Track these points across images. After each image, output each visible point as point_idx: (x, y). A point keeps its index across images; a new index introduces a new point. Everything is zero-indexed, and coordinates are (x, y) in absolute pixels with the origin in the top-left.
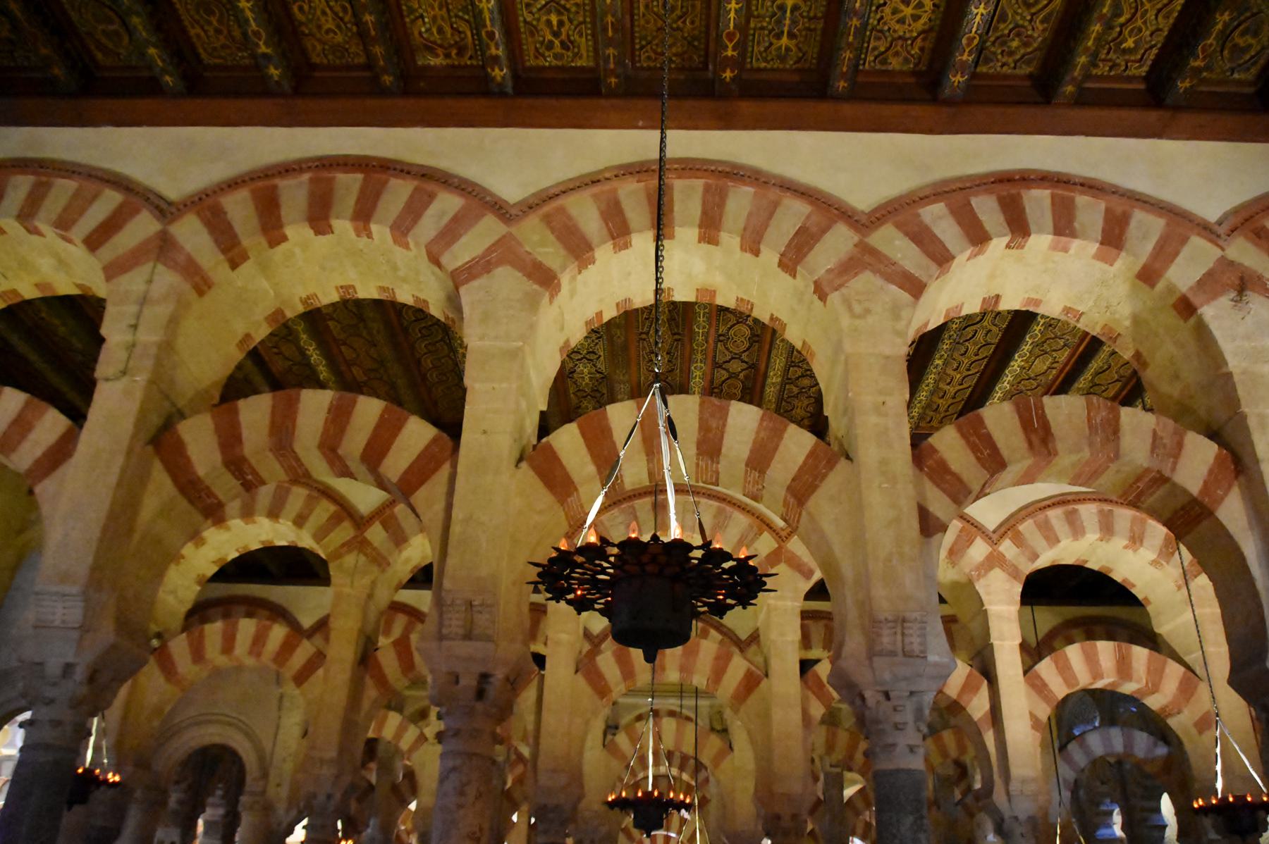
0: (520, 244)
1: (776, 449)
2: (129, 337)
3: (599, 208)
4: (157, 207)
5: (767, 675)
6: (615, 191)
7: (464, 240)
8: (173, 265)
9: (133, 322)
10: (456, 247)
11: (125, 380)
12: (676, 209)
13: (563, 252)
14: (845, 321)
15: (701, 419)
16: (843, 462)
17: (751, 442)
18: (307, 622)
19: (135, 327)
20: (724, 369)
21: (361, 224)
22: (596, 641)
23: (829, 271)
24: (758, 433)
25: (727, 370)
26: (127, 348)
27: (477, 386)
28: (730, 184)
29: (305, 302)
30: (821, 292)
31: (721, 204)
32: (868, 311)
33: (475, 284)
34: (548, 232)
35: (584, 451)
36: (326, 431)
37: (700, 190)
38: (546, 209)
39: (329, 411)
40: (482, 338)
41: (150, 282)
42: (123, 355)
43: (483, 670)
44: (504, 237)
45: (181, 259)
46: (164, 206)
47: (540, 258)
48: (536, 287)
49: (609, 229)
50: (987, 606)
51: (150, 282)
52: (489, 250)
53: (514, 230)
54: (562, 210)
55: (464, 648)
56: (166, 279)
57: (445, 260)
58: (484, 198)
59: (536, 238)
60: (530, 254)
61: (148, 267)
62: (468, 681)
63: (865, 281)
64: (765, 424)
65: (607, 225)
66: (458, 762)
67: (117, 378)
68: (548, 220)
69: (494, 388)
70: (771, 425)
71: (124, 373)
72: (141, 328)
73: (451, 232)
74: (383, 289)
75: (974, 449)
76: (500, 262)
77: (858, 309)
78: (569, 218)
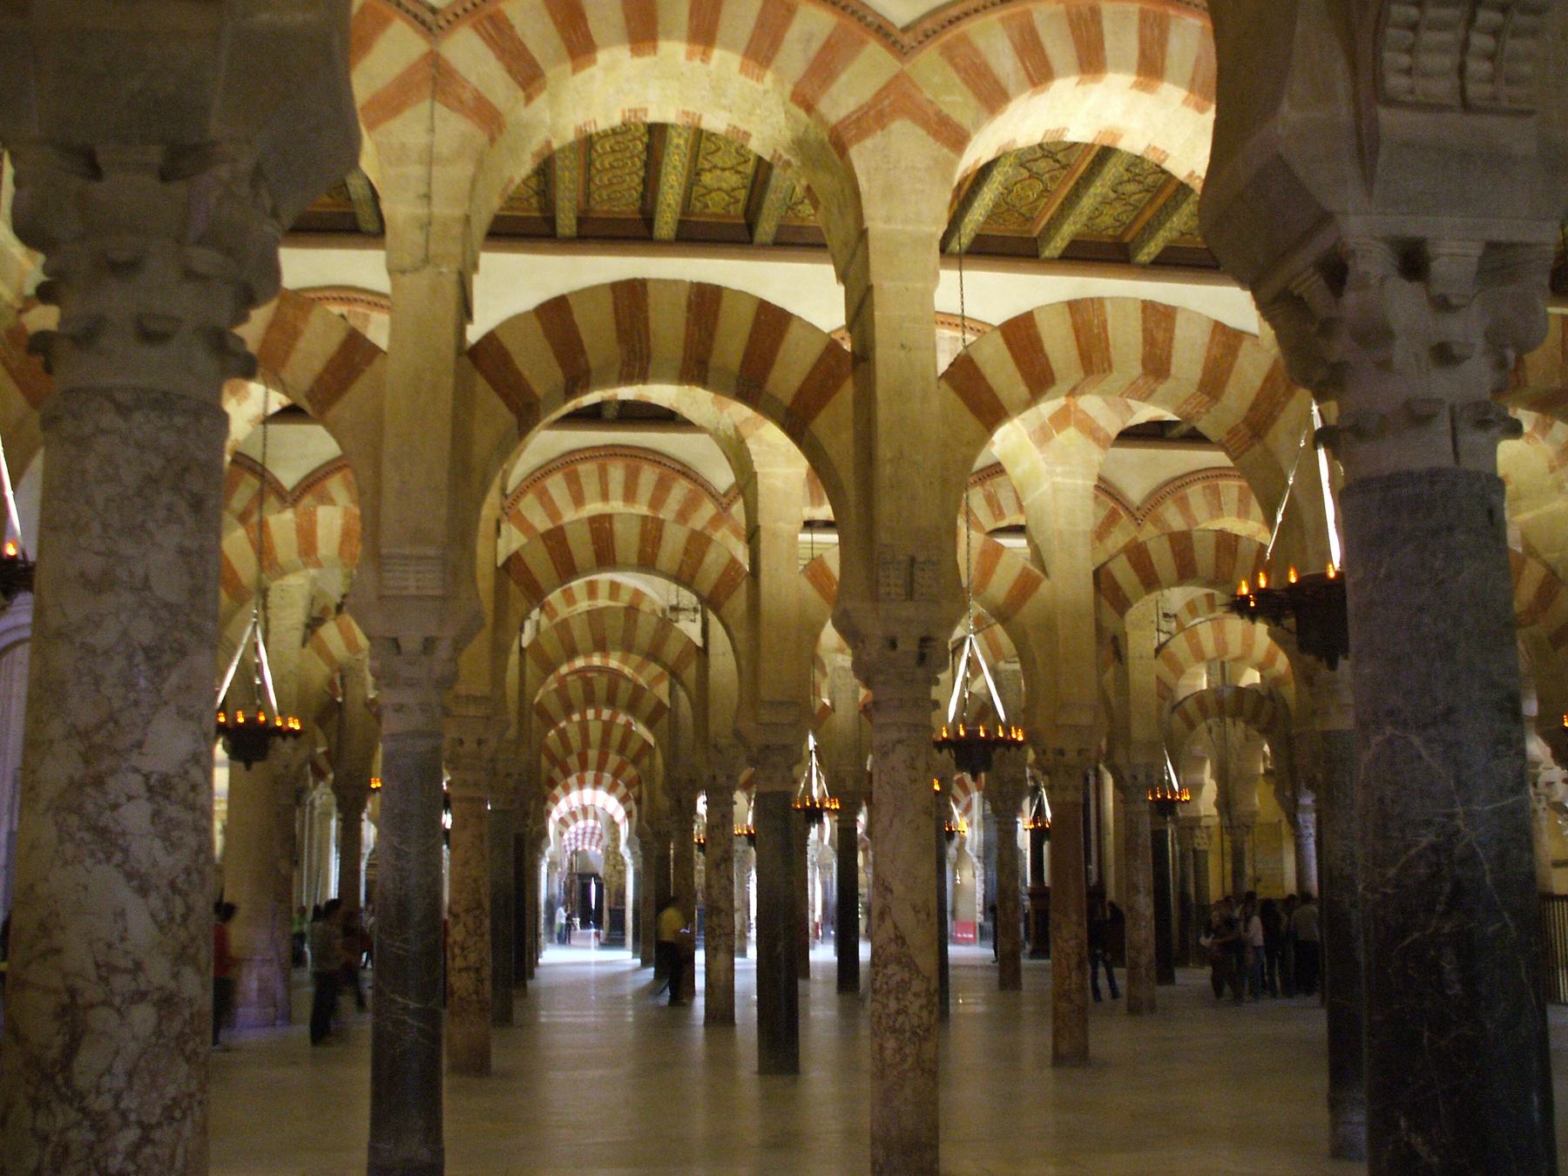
0: (919, 89)
1: (1229, 370)
2: (421, 211)
3: (1011, 37)
4: (416, 16)
6: (1028, 14)
7: (844, 78)
8: (458, 106)
9: (423, 190)
10: (835, 88)
11: (429, 271)
12: (1107, 45)
13: (973, 102)
15: (1144, 330)
17: (1203, 360)
18: (289, 478)
19: (427, 197)
20: (1026, 168)
21: (699, 48)
22: (724, 501)
24: (1209, 350)
25: (1029, 170)
26: (421, 228)
27: (887, 284)
28: (1171, 12)
29: (579, 130)
31: (1162, 43)
33: (869, 143)
34: (953, 74)
35: (1011, 366)
36: (689, 336)
37: (1135, 19)
38: (948, 36)
39: (689, 307)
40: (888, 220)
41: (432, 130)
42: (417, 237)
43: (924, 634)
44: (897, 77)
45: (467, 96)
46: (428, 17)
47: (946, 110)
48: (945, 150)
49: (1026, 69)
51: (432, 130)
52: (879, 96)
53: (907, 67)
54: (964, 39)
56: (454, 128)
57: (824, 106)
58: (865, 17)
59: (937, 79)
60: (932, 103)
61: (424, 107)
62: (908, 646)
64: (1217, 338)
65: (1024, 64)
66: (904, 734)
67: (416, 270)
68: (948, 52)
69: (907, 289)
70: (1224, 339)
72: (435, 200)
73: (824, 67)
74: (686, 113)
76: (898, 111)
78: (976, 51)
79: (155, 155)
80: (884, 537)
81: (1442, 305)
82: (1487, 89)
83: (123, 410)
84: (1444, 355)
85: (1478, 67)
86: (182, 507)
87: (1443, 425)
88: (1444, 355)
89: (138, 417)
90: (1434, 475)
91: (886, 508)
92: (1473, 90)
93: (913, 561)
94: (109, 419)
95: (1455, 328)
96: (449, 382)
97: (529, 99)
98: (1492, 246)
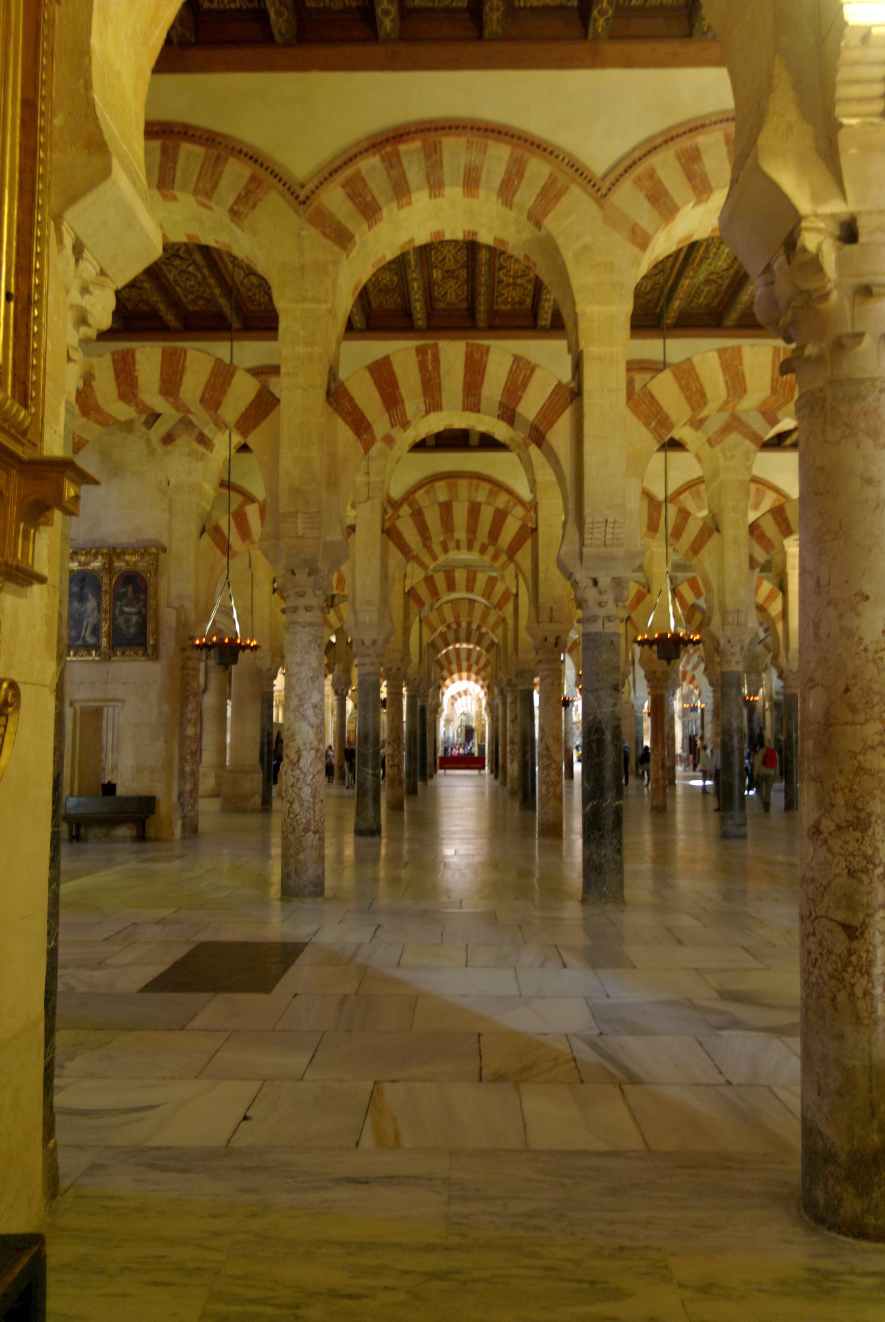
5: (649, 591)
9: (366, 470)
11: (369, 503)
14: (722, 462)
16: (716, 534)
19: (368, 473)
23: (715, 432)
30: (709, 441)
32: (733, 456)
50: (786, 548)
55: (550, 626)
63: (734, 438)
67: (365, 502)
71: (369, 498)
75: (779, 525)
77: (728, 454)
79: (307, 571)
80: (541, 600)
81: (600, 592)
82: (611, 542)
83: (304, 627)
84: (600, 604)
85: (609, 536)
86: (317, 647)
87: (600, 622)
88: (600, 604)
89: (306, 628)
90: (597, 634)
91: (542, 589)
92: (607, 543)
93: (552, 609)
94: (300, 629)
95: (604, 598)
96: (379, 545)
97: (405, 431)
98: (614, 579)
